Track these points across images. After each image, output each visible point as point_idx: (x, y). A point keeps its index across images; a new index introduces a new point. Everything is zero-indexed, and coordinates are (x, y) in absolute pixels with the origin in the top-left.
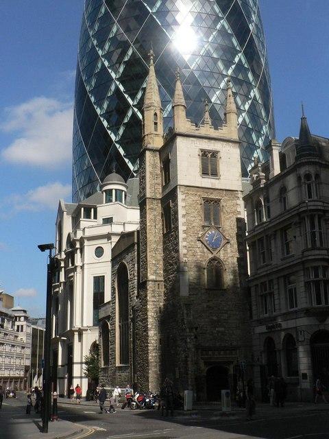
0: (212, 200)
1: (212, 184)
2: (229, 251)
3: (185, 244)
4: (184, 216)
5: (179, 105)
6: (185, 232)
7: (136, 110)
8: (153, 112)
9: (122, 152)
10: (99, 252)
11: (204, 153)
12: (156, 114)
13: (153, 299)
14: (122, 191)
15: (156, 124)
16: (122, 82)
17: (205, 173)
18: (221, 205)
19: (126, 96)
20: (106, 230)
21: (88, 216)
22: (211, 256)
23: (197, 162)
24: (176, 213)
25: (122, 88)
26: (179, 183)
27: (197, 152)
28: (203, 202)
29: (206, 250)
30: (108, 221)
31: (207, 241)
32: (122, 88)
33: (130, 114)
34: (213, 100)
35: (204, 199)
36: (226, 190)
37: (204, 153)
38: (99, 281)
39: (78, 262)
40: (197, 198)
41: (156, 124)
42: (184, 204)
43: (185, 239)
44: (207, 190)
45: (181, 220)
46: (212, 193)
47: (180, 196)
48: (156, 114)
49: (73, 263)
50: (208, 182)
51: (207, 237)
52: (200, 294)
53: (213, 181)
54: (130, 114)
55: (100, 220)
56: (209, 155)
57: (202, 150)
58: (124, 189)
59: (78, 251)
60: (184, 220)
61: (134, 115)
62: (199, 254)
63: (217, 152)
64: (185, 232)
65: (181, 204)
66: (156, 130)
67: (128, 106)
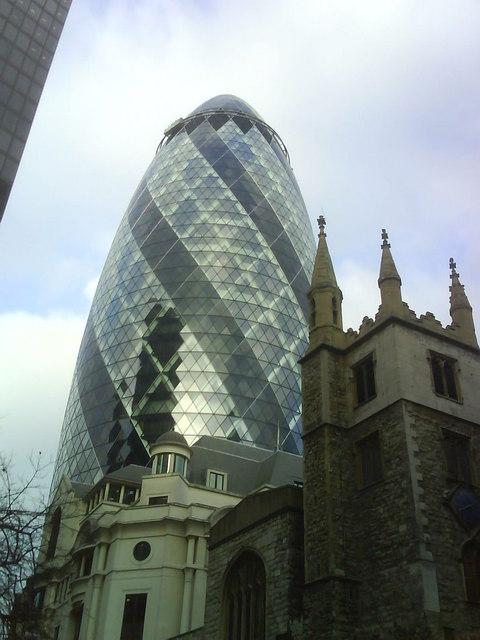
0: (456, 436)
1: (452, 409)
3: (423, 506)
4: (417, 454)
6: (421, 483)
7: (166, 378)
8: (330, 295)
9: (140, 432)
10: (142, 551)
13: (343, 618)
14: (185, 457)
16: (150, 343)
17: (439, 390)
18: (471, 449)
19: (155, 360)
20: (157, 513)
21: (114, 496)
23: (427, 369)
24: (403, 446)
25: (150, 350)
27: (424, 354)
28: (442, 437)
29: (457, 525)
30: (157, 501)
32: (150, 350)
33: (157, 383)
34: (270, 379)
37: (434, 359)
38: (136, 606)
39: (98, 566)
40: (431, 428)
42: (414, 433)
43: (423, 498)
45: (414, 462)
47: (409, 420)
49: (87, 571)
50: (443, 405)
52: (456, 610)
53: (454, 405)
54: (157, 383)
55: (145, 500)
56: (443, 363)
57: (432, 352)
58: (188, 456)
59: (103, 550)
60: (418, 462)
61: (162, 385)
62: (447, 530)
64: (421, 483)
65: (410, 433)
67: (156, 373)
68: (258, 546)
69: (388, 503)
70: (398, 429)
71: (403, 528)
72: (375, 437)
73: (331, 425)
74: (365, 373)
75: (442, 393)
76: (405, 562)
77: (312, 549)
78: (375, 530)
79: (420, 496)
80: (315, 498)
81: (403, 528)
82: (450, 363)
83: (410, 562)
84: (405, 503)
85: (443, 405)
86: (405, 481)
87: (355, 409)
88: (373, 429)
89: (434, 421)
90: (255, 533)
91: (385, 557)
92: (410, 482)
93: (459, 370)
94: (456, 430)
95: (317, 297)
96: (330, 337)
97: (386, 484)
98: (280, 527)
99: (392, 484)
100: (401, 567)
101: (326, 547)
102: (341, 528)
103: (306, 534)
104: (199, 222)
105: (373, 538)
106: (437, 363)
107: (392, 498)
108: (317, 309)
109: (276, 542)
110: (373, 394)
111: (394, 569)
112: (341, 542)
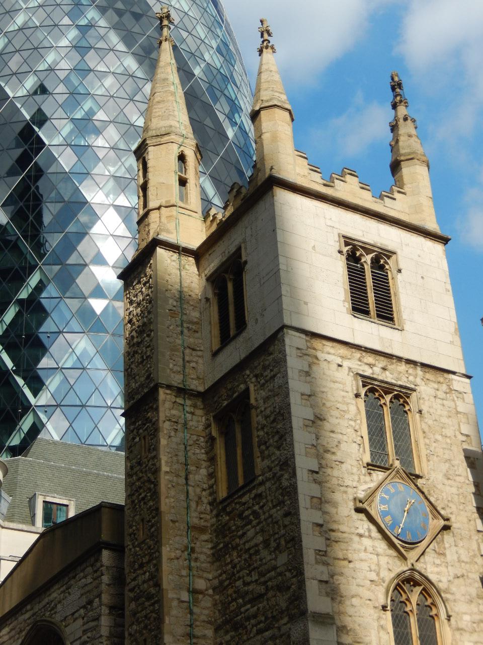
0: (388, 388)
1: (381, 339)
2: (451, 556)
5: (275, 106)
8: (175, 151)
11: (353, 252)
12: (182, 158)
15: (183, 182)
17: (359, 307)
22: (400, 567)
23: (339, 269)
26: (287, 321)
27: (334, 244)
31: (384, 514)
35: (366, 380)
36: (423, 365)
37: (353, 252)
41: (183, 182)
44: (370, 359)
46: (384, 369)
48: (182, 158)
51: (383, 501)
56: (367, 259)
57: (348, 241)
63: (389, 254)
66: (183, 197)
68: (58, 618)
69: (263, 517)
70: (278, 381)
71: (283, 559)
72: (242, 404)
73: (169, 387)
74: (230, 286)
75: (366, 313)
76: (286, 620)
77: (134, 614)
78: (241, 569)
79: (312, 497)
80: (143, 520)
81: (283, 559)
82: (381, 258)
83: (292, 619)
84: (287, 514)
85: (368, 332)
86: (286, 476)
87: (215, 354)
88: (243, 387)
89: (346, 364)
90: (55, 595)
91: (255, 616)
92: (294, 475)
93: (400, 271)
94: (389, 377)
95: (152, 154)
96: (171, 226)
97: (262, 483)
98: (89, 580)
99: (268, 484)
100: (279, 628)
101: (157, 606)
102: (184, 572)
103: (127, 588)
104: (42, 67)
105: (239, 583)
106: (357, 260)
107: (266, 508)
108: (150, 175)
109: (84, 607)
110: (241, 324)
111: (267, 634)
112: (185, 596)
